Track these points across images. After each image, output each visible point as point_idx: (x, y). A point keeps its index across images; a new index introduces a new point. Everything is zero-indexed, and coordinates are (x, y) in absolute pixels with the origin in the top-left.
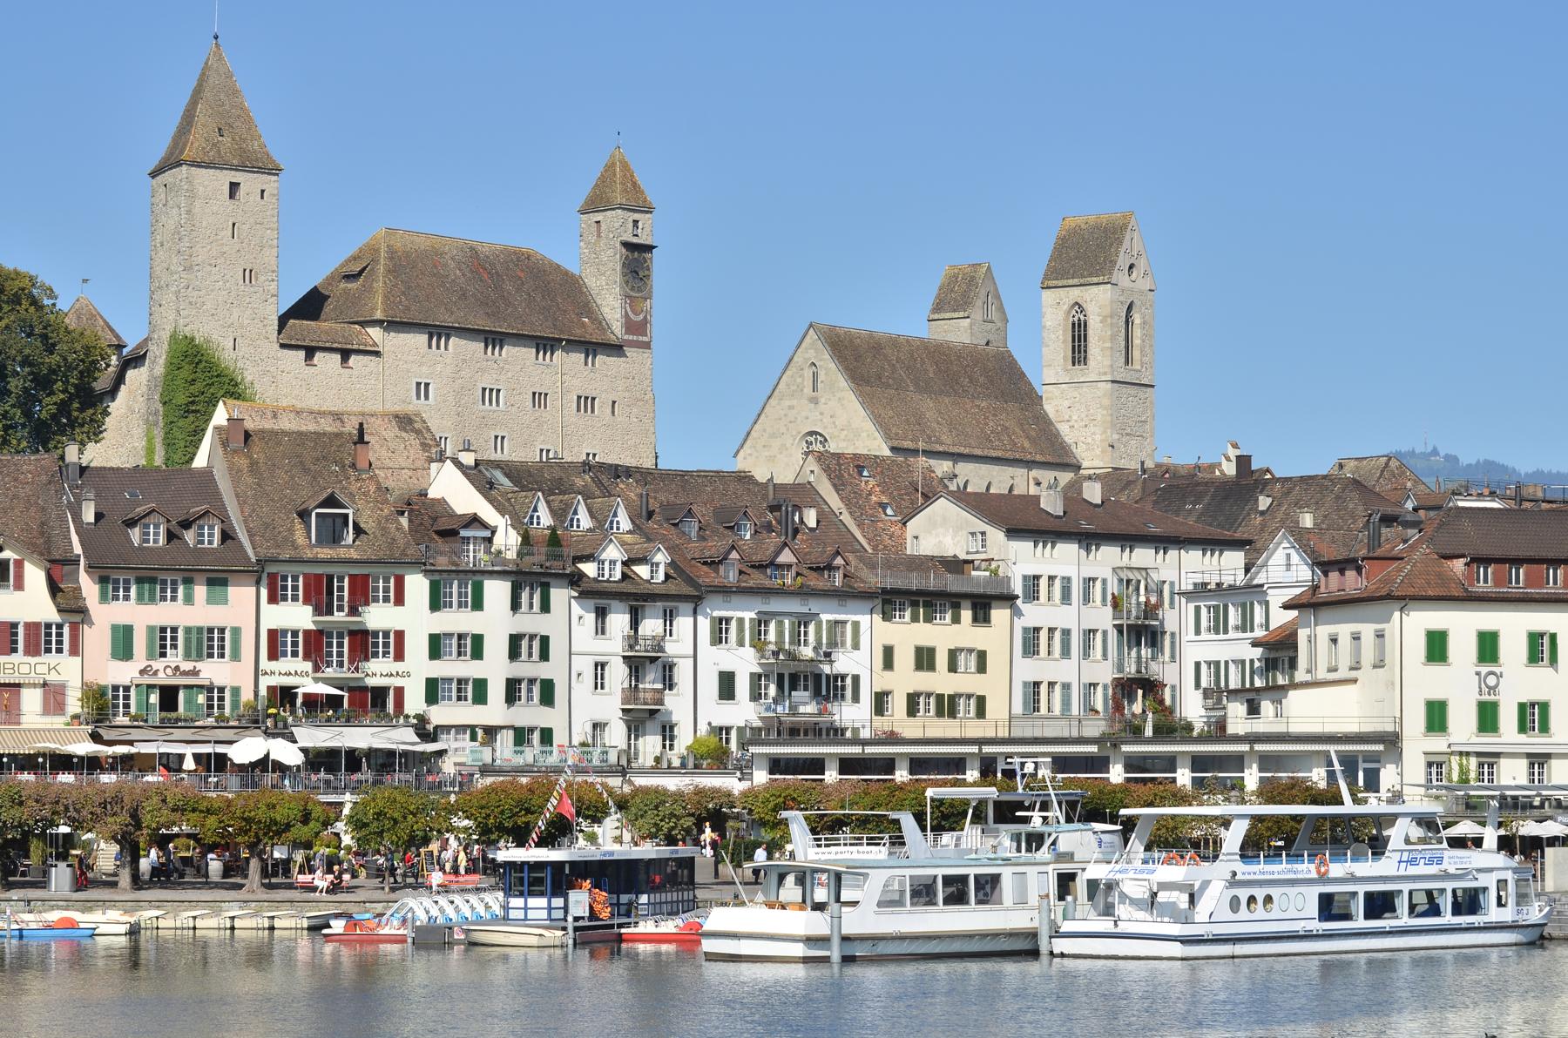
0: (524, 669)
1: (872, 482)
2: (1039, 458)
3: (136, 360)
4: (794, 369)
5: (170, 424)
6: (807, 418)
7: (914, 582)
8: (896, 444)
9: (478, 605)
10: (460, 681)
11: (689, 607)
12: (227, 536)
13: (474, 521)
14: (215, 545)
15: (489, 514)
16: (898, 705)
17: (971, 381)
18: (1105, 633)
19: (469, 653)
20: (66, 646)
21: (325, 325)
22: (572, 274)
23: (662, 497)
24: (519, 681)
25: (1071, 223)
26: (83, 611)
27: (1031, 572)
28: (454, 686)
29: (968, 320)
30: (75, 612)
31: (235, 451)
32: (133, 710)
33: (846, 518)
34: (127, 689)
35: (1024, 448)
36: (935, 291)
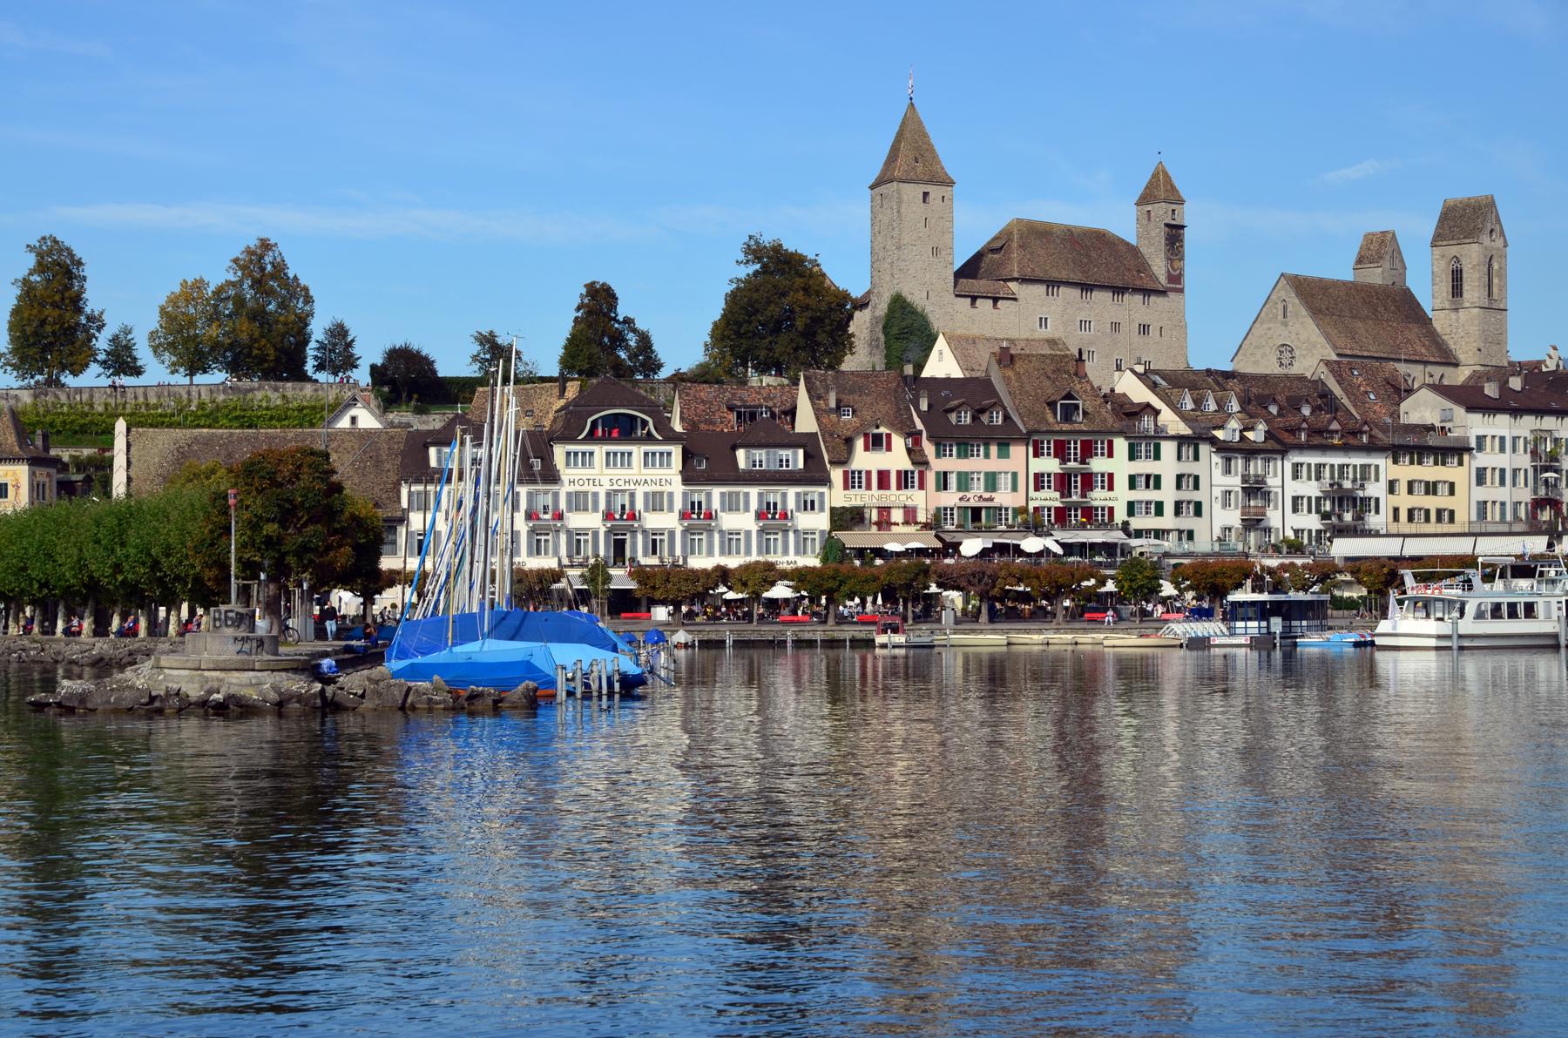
0: (1188, 495)
1: (1360, 379)
2: (1432, 359)
3: (861, 305)
5: (888, 347)
7: (1411, 440)
8: (1340, 351)
9: (1157, 457)
10: (1147, 503)
11: (1279, 457)
12: (1007, 417)
13: (1148, 405)
15: (1157, 403)
16: (1403, 515)
18: (1526, 471)
20: (916, 484)
21: (983, 282)
23: (1254, 390)
24: (1182, 502)
26: (926, 463)
27: (1481, 433)
28: (1144, 505)
30: (920, 461)
31: (1005, 367)
32: (956, 521)
34: (952, 509)
36: (1357, 250)
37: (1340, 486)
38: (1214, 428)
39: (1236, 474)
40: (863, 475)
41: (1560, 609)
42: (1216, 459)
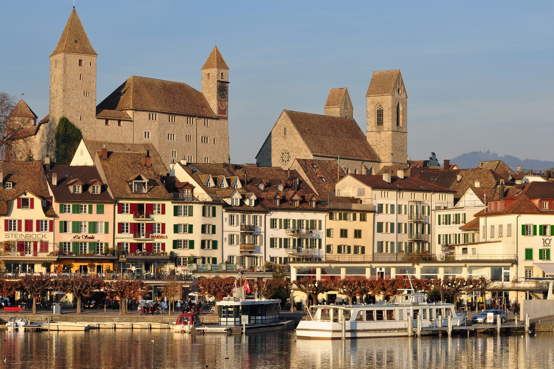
0: (207, 237)
1: (317, 170)
4: (277, 127)
5: (58, 146)
6: (282, 144)
7: (340, 206)
9: (191, 215)
10: (184, 241)
13: (187, 185)
14: (99, 193)
15: (192, 181)
16: (335, 249)
17: (341, 131)
18: (406, 224)
19: (188, 231)
22: (200, 93)
26: (55, 216)
28: (182, 243)
29: (339, 109)
31: (104, 160)
34: (69, 243)
35: (360, 155)
36: (327, 98)
37: (298, 231)
38: (225, 198)
40: (17, 223)
41: (408, 314)
42: (226, 215)
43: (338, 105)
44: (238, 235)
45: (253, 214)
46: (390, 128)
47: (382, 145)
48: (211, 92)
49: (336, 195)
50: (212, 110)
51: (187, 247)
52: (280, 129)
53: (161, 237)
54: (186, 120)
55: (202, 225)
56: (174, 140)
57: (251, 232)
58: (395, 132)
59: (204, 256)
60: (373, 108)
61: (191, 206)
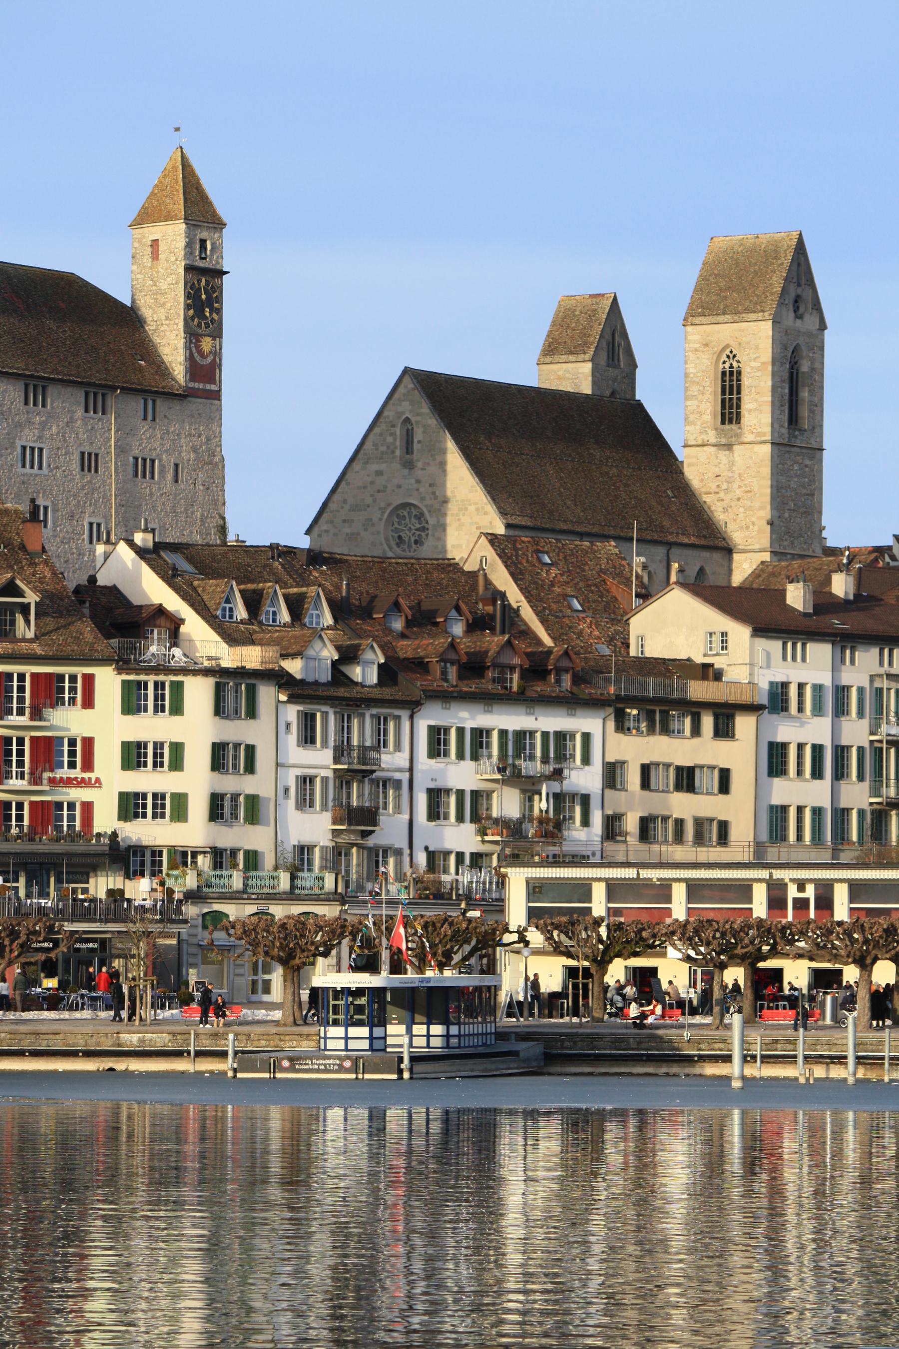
0: (229, 784)
1: (554, 571)
4: (383, 426)
7: (651, 687)
9: (177, 709)
10: (155, 796)
11: (404, 714)
13: (160, 611)
18: (861, 750)
25: (722, 242)
28: (149, 802)
33: (528, 614)
39: (325, 745)
42: (292, 713)
43: (585, 353)
44: (327, 778)
45: (374, 711)
46: (764, 434)
47: (738, 493)
48: (164, 304)
49: (633, 652)
50: (167, 368)
51: (163, 816)
52: (391, 434)
53: (78, 783)
54: (83, 400)
55: (214, 744)
56: (40, 468)
57: (368, 768)
58: (782, 448)
59: (220, 844)
60: (706, 362)
61: (178, 682)
